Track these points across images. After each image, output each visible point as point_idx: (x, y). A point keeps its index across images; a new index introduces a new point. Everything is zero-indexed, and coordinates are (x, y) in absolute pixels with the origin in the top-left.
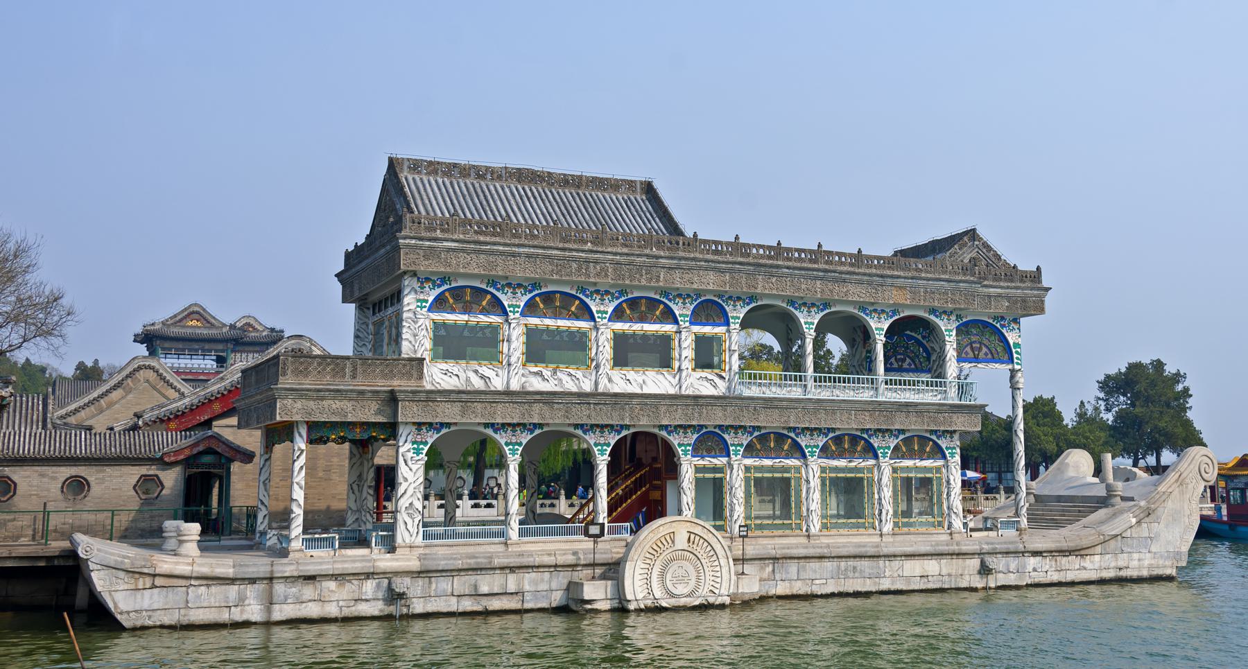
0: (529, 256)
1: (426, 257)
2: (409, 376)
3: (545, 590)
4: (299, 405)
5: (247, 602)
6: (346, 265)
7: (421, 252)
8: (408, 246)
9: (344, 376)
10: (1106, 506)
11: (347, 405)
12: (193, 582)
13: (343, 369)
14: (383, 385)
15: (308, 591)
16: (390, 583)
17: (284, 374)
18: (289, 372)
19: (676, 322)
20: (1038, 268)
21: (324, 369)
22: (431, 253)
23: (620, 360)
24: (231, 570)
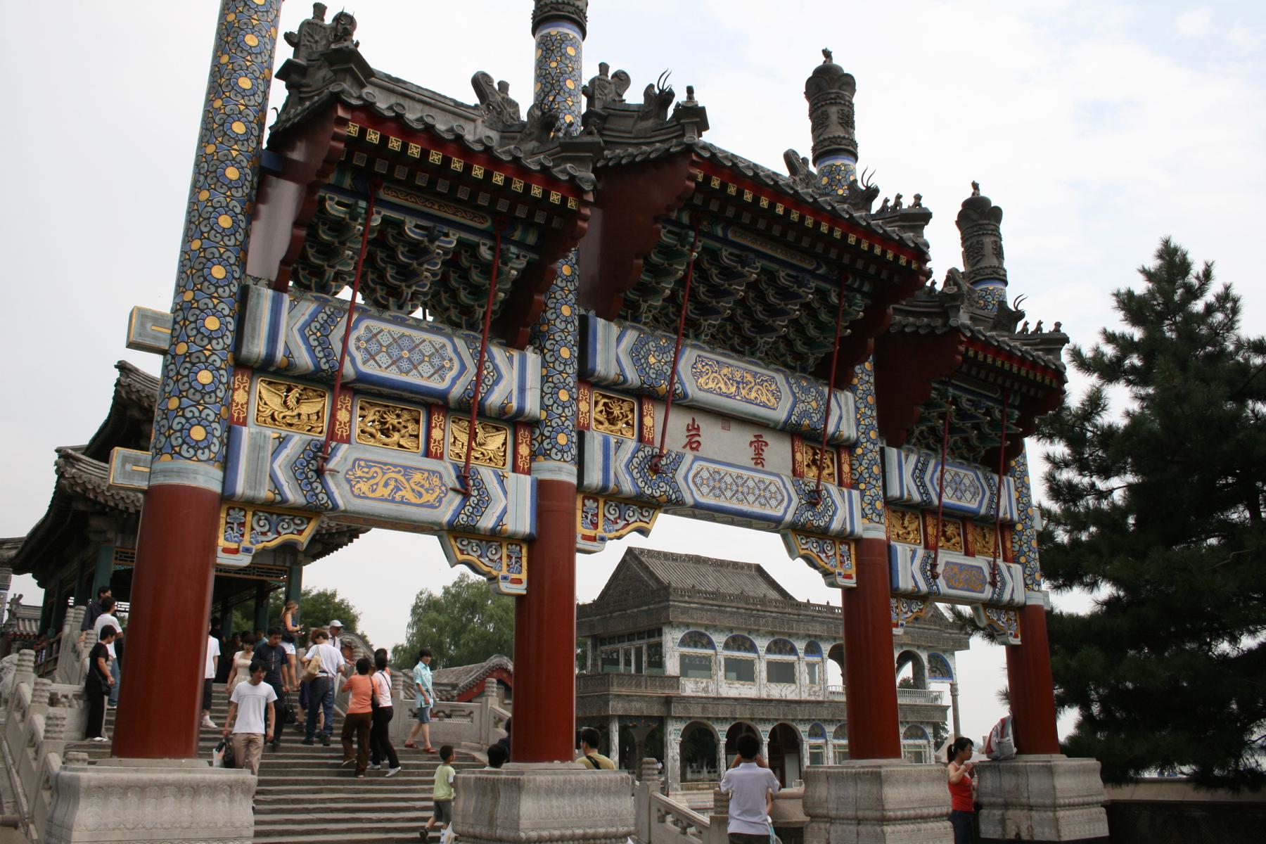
0: (731, 613)
2: (672, 687)
6: (300, 572)
11: (644, 705)
14: (661, 692)
19: (796, 654)
22: (685, 611)
23: (770, 680)
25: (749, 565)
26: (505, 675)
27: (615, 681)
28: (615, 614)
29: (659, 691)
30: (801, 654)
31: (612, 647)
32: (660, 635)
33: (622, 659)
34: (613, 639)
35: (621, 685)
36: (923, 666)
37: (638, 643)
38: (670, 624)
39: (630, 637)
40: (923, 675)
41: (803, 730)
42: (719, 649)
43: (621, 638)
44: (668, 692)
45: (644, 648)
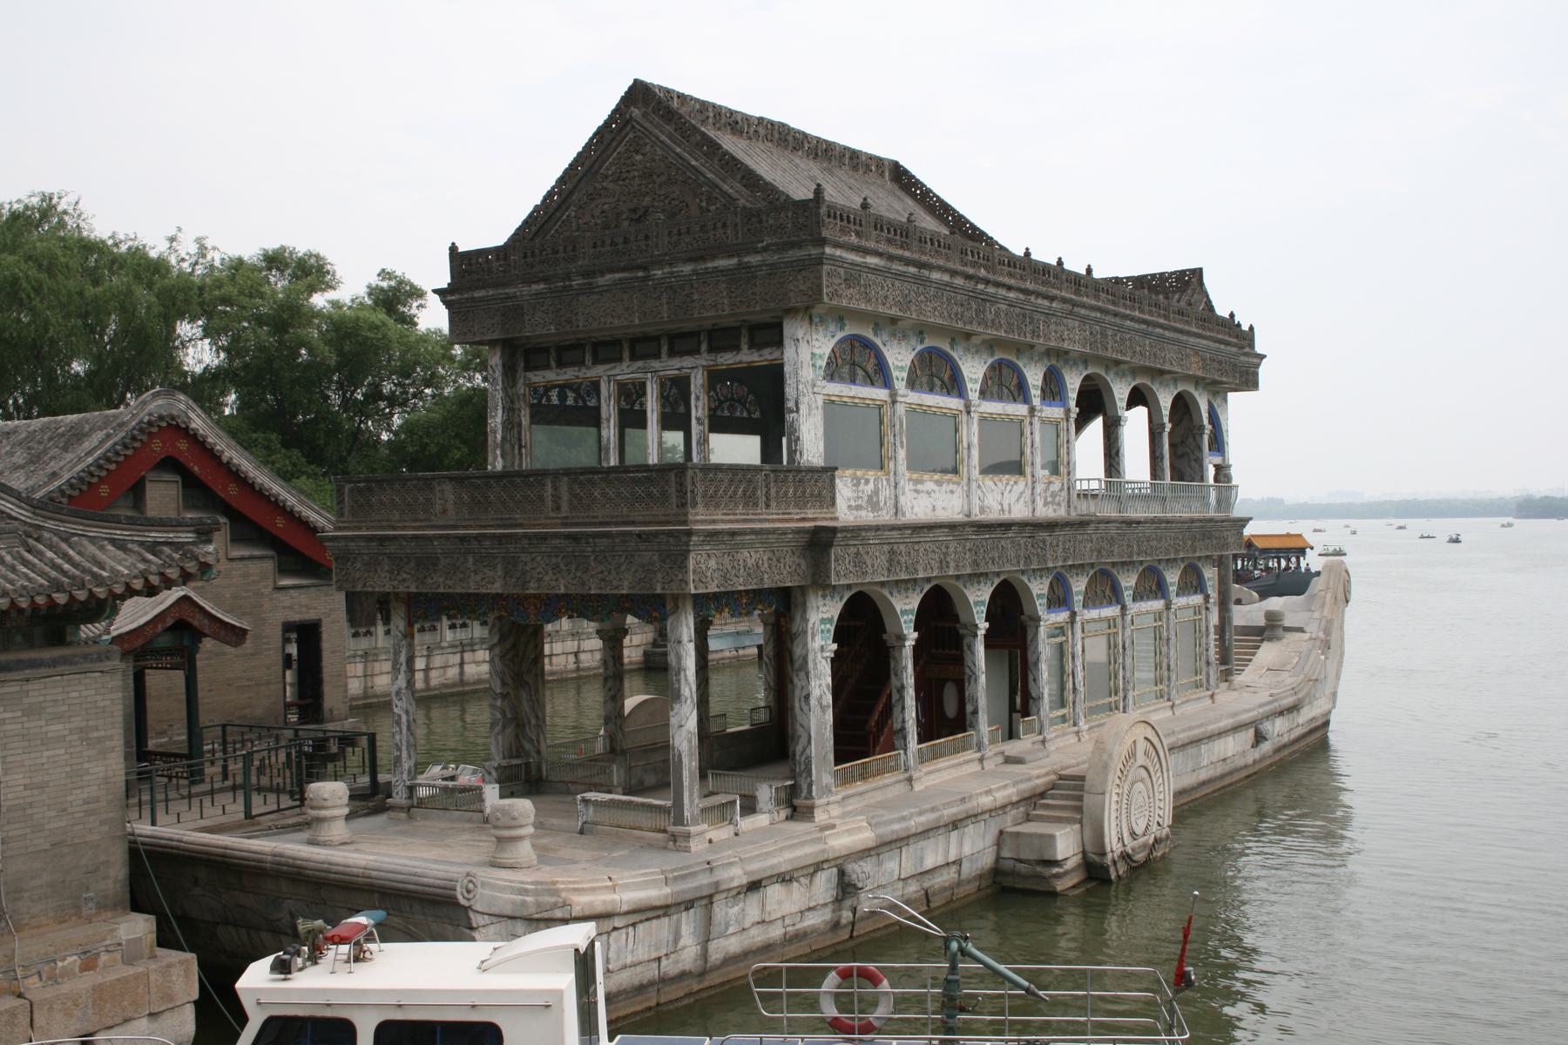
1: (850, 281)
3: (974, 849)
4: (712, 563)
5: (680, 945)
7: (842, 271)
8: (833, 258)
9: (756, 505)
10: (1270, 639)
12: (618, 922)
13: (754, 492)
15: (751, 908)
16: (842, 873)
17: (695, 505)
18: (699, 499)
20: (1251, 328)
21: (735, 492)
24: (667, 890)
25: (879, 162)
26: (183, 445)
27: (700, 489)
28: (602, 281)
29: (796, 514)
30: (1036, 402)
31: (569, 374)
32: (779, 343)
33: (609, 411)
34: (568, 352)
35: (712, 501)
36: (1202, 427)
37: (672, 366)
39: (643, 346)
40: (1200, 448)
41: (1039, 588)
42: (900, 386)
43: (606, 349)
44: (814, 517)
45: (698, 382)
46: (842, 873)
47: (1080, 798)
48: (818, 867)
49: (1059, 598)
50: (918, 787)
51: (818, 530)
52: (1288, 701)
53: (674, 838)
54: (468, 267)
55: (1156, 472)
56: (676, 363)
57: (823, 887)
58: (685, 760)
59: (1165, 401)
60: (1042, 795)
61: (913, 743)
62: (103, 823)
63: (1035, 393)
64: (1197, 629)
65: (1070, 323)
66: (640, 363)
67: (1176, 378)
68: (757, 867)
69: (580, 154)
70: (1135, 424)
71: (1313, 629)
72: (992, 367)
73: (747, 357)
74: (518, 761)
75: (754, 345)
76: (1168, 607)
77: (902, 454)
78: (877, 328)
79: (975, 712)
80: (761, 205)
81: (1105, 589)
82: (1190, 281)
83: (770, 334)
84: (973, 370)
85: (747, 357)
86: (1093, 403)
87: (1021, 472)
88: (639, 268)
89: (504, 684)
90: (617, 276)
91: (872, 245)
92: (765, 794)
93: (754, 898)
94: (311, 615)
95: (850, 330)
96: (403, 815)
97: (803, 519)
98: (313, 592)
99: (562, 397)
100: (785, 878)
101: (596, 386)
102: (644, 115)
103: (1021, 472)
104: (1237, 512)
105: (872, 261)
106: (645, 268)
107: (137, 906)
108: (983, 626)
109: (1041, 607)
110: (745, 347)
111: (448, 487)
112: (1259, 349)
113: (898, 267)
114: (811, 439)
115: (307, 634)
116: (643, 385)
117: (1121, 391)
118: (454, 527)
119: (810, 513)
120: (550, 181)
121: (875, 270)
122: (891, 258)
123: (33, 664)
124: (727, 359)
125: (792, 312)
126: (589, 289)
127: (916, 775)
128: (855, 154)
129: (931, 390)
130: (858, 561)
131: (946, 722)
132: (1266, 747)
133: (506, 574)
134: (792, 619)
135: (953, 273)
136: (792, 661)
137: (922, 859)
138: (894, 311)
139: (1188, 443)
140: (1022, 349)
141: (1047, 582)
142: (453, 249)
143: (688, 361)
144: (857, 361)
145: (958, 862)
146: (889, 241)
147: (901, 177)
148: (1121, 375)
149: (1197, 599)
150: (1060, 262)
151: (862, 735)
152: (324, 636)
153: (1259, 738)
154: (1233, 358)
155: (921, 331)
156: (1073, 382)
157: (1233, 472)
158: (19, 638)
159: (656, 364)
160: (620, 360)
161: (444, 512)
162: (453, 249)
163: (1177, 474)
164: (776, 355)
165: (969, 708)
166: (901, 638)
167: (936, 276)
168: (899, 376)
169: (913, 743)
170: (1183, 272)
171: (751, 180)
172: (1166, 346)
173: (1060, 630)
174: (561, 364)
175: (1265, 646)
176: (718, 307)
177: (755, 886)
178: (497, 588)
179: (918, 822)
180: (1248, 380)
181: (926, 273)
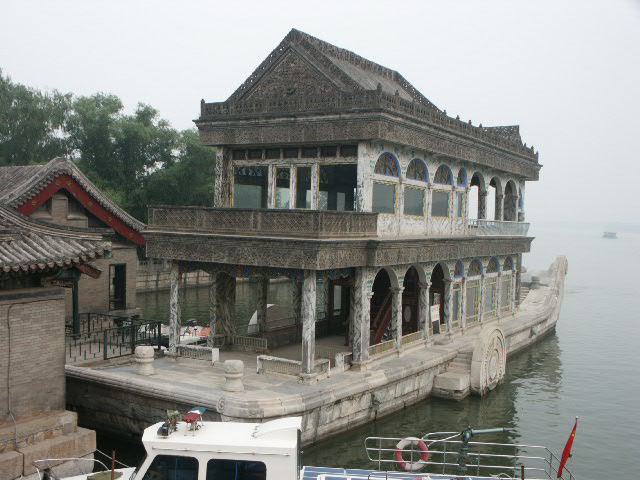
16: (373, 396)
24: (304, 404)
30: (455, 184)
31: (254, 163)
32: (355, 155)
34: (254, 151)
37: (303, 162)
38: (370, 143)
39: (290, 151)
40: (514, 206)
41: (451, 268)
43: (272, 151)
44: (368, 236)
46: (373, 396)
47: (470, 363)
48: (363, 393)
49: (458, 273)
50: (401, 356)
51: (370, 242)
52: (543, 318)
53: (302, 379)
54: (209, 111)
55: (497, 216)
56: (305, 160)
57: (365, 402)
58: (309, 344)
59: (504, 184)
60: (452, 360)
61: (400, 337)
62: (55, 369)
63: (455, 180)
64: (507, 285)
65: (473, 150)
66: (288, 160)
67: (509, 174)
68: (340, 394)
69: (264, 62)
70: (491, 191)
71: (552, 286)
72: (412, 162)
73: (338, 160)
74: (221, 336)
75: (341, 155)
76: (499, 276)
77: (402, 207)
78: (396, 150)
79: (424, 322)
80: (350, 91)
81: (476, 268)
82: (514, 131)
83: (351, 149)
84: (432, 169)
85: (338, 160)
86: (476, 181)
87: (447, 215)
88: (291, 117)
89: (218, 301)
90: (281, 119)
91: (399, 112)
92: (340, 358)
93: (337, 408)
94: (122, 262)
95: (386, 150)
96: (173, 360)
97: (364, 236)
98: (123, 252)
99: (247, 172)
100: (350, 398)
101: (265, 170)
102: (297, 46)
103: (447, 215)
104: (529, 235)
105: (400, 119)
106: (294, 116)
107: (69, 407)
108: (430, 284)
109: (452, 276)
110: (338, 157)
111: (203, 214)
112: (540, 163)
113: (408, 122)
114: (366, 200)
115: (120, 270)
116: (289, 170)
117: (487, 180)
118: (204, 232)
119: (367, 234)
120: (249, 74)
121: (399, 124)
122: (407, 118)
123: (26, 296)
124: (330, 161)
125: (362, 141)
126: (266, 125)
127: (400, 350)
128: (380, 68)
129: (385, 173)
130: (386, 257)
131: (412, 326)
132: (534, 337)
133: (230, 255)
134: (355, 280)
135: (430, 126)
136: (354, 300)
137: (404, 389)
138: (407, 143)
139: (510, 205)
140: (451, 160)
141: (455, 264)
142: (203, 102)
143: (311, 160)
144: (387, 165)
145: (418, 390)
146: (406, 111)
147: (398, 78)
148: (488, 173)
149: (510, 272)
150: (458, 118)
151: (381, 331)
152: (127, 271)
153: (532, 333)
154: (527, 165)
155: (414, 151)
156: (470, 176)
157: (525, 216)
158: (19, 283)
159: (295, 160)
160: (278, 157)
161: (201, 225)
162: (203, 102)
163: (505, 219)
164: (353, 160)
165: (421, 320)
166: (398, 290)
167: (424, 127)
168: (403, 171)
169: (400, 337)
170: (510, 127)
171: (346, 79)
172: (502, 159)
173: (457, 286)
174: (250, 157)
175: (531, 292)
176: (329, 135)
177: (338, 402)
178: (225, 261)
179: (404, 372)
180: (535, 177)
181: (419, 126)
